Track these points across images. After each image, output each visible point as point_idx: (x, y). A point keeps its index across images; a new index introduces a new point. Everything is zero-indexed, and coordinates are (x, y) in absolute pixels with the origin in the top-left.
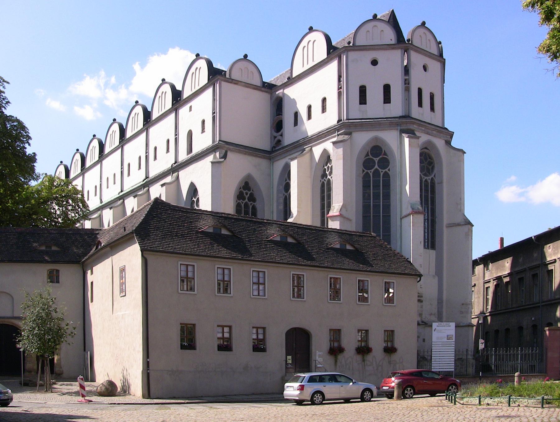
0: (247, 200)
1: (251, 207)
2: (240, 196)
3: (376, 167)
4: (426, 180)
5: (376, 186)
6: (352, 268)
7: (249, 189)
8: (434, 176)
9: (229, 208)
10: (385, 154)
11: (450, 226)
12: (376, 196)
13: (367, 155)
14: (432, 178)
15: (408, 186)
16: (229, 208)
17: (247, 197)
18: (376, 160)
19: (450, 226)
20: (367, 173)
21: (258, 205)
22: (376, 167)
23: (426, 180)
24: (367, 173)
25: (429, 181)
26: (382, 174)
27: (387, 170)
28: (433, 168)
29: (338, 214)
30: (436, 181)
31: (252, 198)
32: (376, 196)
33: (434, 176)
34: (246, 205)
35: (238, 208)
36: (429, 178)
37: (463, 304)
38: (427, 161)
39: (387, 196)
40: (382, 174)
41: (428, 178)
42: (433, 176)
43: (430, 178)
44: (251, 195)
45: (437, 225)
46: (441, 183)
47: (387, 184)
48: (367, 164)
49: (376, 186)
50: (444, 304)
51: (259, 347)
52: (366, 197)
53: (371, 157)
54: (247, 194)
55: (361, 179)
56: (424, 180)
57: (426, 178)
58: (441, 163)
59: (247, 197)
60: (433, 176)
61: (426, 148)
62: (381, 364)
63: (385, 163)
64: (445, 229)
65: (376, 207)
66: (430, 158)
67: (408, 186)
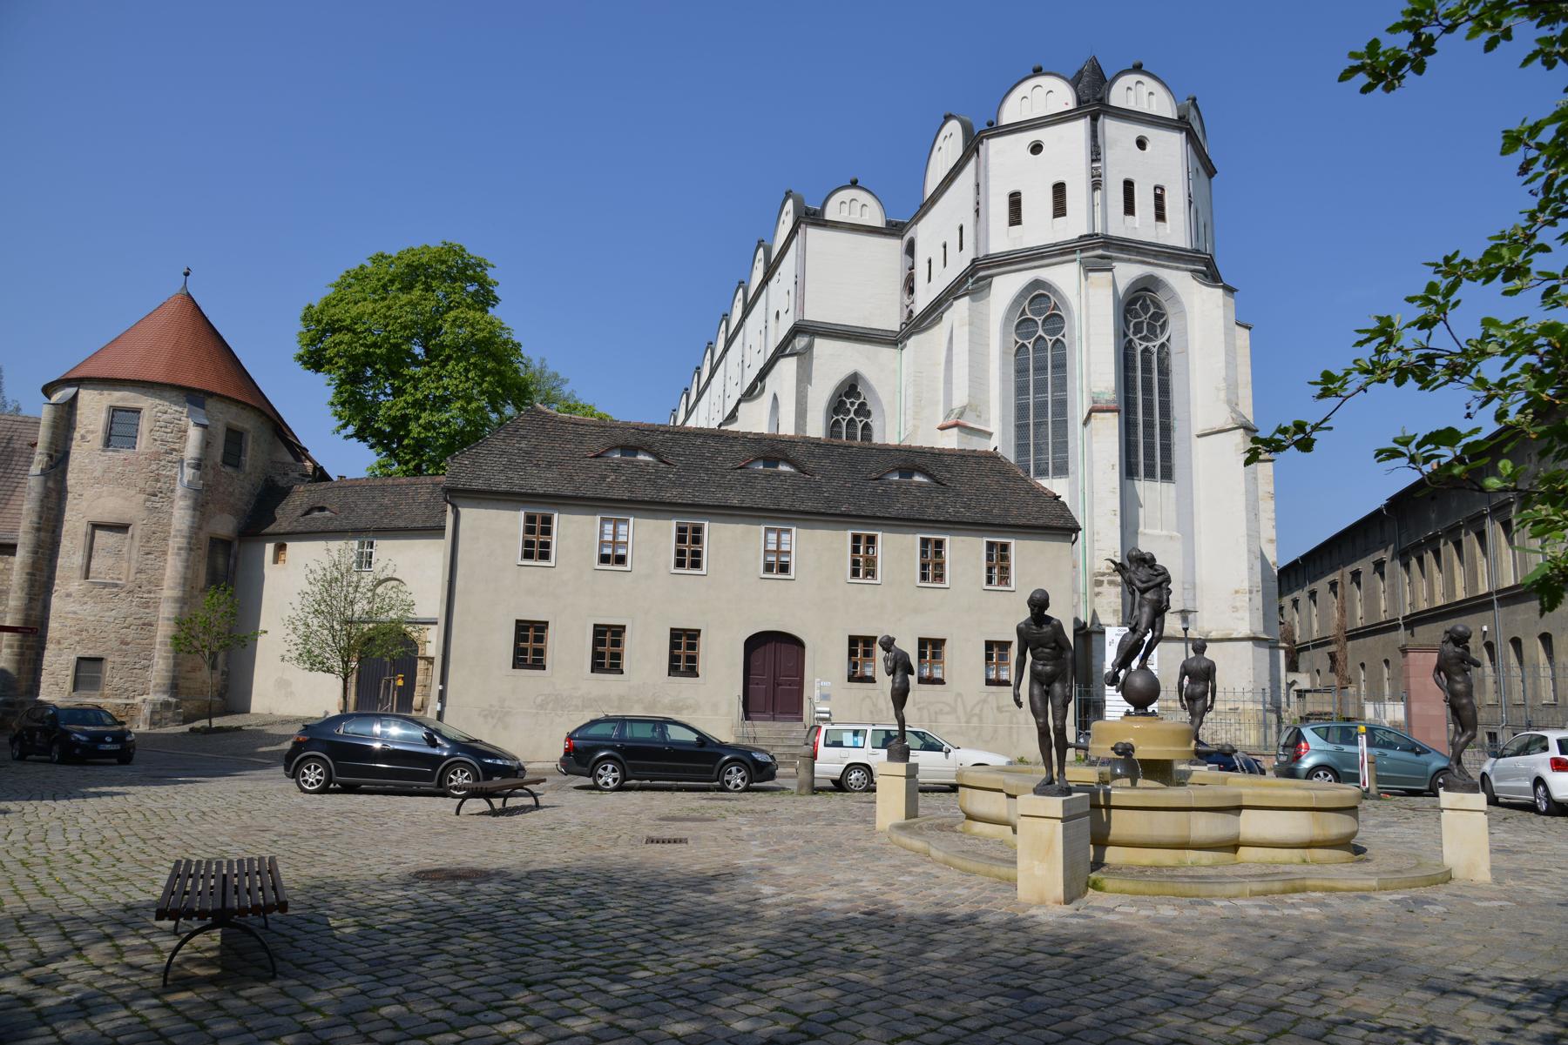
1: (860, 426)
2: (837, 406)
3: (1040, 332)
5: (1041, 369)
9: (816, 428)
10: (1056, 307)
14: (1163, 345)
16: (816, 428)
20: (1023, 345)
23: (1146, 350)
24: (1023, 345)
31: (863, 410)
32: (1041, 387)
34: (851, 422)
36: (1154, 345)
39: (1061, 384)
41: (1150, 345)
42: (1164, 340)
43: (1158, 343)
44: (863, 405)
46: (1184, 351)
47: (1061, 366)
49: (1041, 369)
52: (1021, 389)
54: (852, 404)
58: (1182, 313)
62: (977, 711)
63: (1055, 321)
65: (1041, 407)
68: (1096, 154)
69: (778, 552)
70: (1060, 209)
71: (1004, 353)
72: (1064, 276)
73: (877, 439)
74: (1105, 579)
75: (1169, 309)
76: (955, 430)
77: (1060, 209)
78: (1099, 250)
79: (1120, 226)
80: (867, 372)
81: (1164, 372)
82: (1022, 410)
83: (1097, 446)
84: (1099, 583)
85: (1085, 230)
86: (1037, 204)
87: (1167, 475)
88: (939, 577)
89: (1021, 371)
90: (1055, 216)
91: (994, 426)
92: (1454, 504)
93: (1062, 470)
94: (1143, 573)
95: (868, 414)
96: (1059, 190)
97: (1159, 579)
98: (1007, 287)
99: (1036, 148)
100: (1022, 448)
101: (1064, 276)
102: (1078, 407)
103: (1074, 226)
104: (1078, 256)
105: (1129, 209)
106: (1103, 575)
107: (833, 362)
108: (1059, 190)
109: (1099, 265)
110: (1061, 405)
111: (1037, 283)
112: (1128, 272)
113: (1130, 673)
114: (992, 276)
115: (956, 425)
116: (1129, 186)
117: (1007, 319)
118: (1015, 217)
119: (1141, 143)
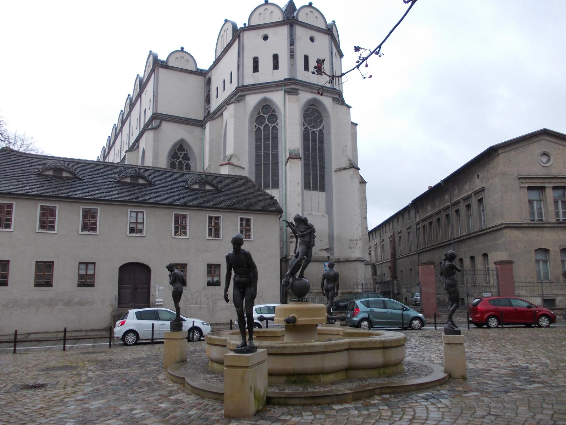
0: (181, 159)
3: (267, 122)
4: (313, 132)
5: (266, 139)
6: (195, 203)
7: (184, 150)
8: (323, 128)
10: (274, 111)
11: (337, 171)
12: (267, 147)
13: (259, 113)
15: (291, 136)
17: (181, 157)
18: (266, 116)
19: (337, 171)
20: (259, 128)
21: (192, 163)
22: (267, 122)
23: (313, 132)
24: (259, 128)
25: (317, 132)
26: (271, 128)
27: (275, 124)
28: (322, 120)
29: (227, 162)
30: (325, 132)
31: (186, 157)
32: (267, 147)
33: (323, 128)
35: (172, 165)
37: (351, 240)
38: (313, 115)
39: (276, 147)
40: (271, 128)
41: (315, 130)
42: (321, 128)
43: (318, 129)
45: (326, 170)
46: (329, 134)
47: (276, 138)
48: (259, 119)
49: (266, 139)
50: (335, 240)
51: (86, 281)
52: (258, 148)
53: (262, 114)
54: (181, 154)
55: (254, 134)
56: (311, 131)
57: (313, 129)
58: (328, 116)
59: (181, 157)
60: (321, 128)
61: (313, 105)
63: (274, 117)
64: (333, 173)
65: (267, 156)
67: (291, 136)
68: (292, 43)
69: (137, 223)
70: (276, 66)
71: (250, 131)
72: (277, 97)
73: (192, 169)
76: (227, 166)
77: (276, 66)
78: (291, 86)
79: (302, 75)
80: (189, 139)
81: (322, 141)
82: (258, 157)
83: (292, 174)
85: (286, 76)
86: (266, 63)
87: (322, 189)
88: (217, 235)
89: (258, 139)
90: (274, 69)
91: (245, 165)
92: (437, 203)
93: (276, 185)
94: (302, 228)
95: (188, 159)
96: (275, 58)
97: (309, 230)
98: (253, 100)
99: (266, 38)
100: (258, 175)
101: (277, 97)
102: (283, 155)
103: (282, 74)
104: (283, 88)
105: (306, 68)
107: (172, 134)
108: (275, 58)
109: (293, 92)
110: (276, 156)
111: (265, 100)
112: (305, 96)
113: (295, 279)
114: (245, 95)
115: (228, 164)
116: (306, 58)
117: (251, 116)
118: (256, 68)
119: (312, 39)
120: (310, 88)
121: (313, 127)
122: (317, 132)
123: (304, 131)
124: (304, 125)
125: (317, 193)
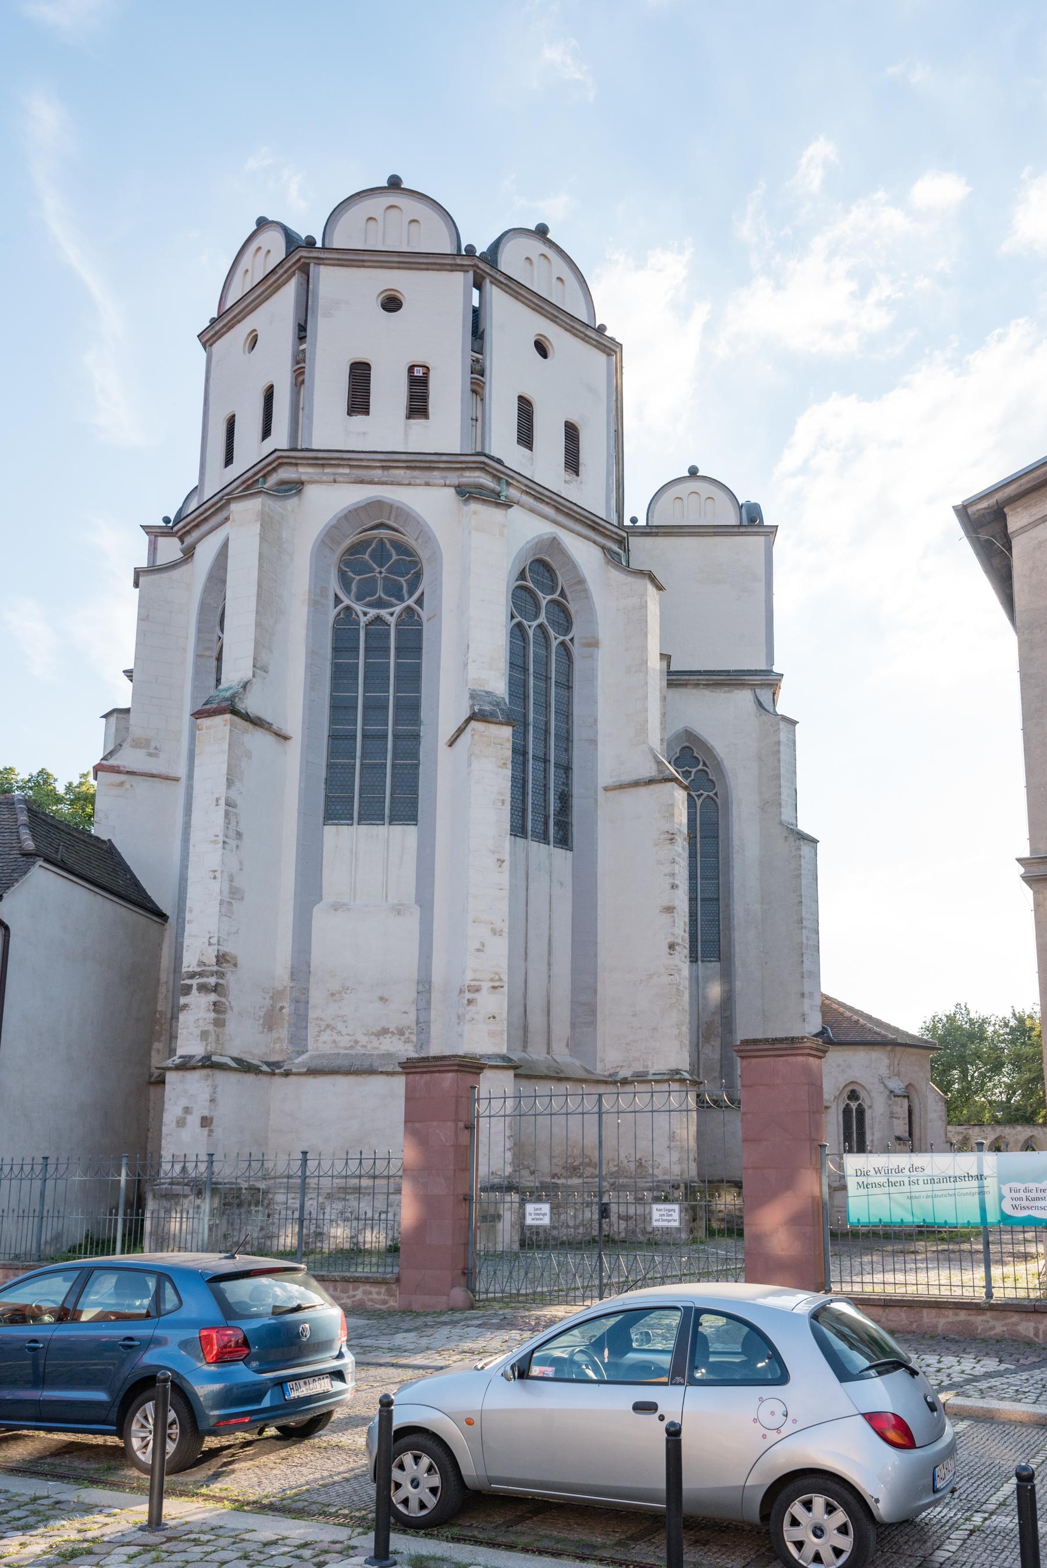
4: (378, 619)
8: (420, 602)
23: (378, 619)
25: (392, 620)
28: (418, 576)
30: (424, 615)
41: (383, 612)
43: (398, 609)
56: (363, 620)
57: (373, 612)
60: (411, 602)
66: (403, 549)
74: (194, 982)
75: (423, 554)
84: (187, 990)
99: (253, 341)
105: (359, 400)
106: (192, 975)
120: (351, 466)
121: (380, 604)
122: (392, 620)
123: (337, 621)
124: (338, 600)
125: (382, 831)
